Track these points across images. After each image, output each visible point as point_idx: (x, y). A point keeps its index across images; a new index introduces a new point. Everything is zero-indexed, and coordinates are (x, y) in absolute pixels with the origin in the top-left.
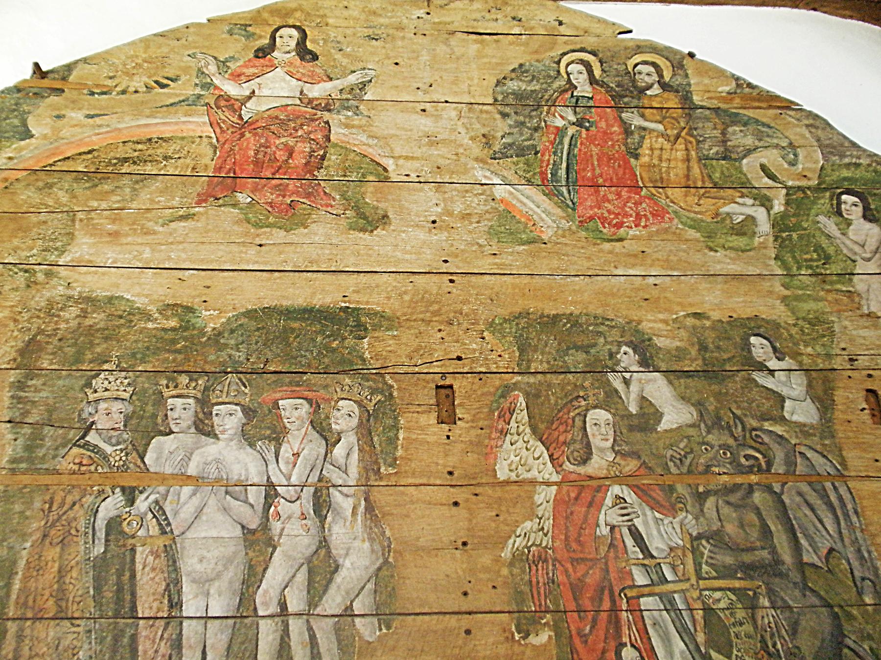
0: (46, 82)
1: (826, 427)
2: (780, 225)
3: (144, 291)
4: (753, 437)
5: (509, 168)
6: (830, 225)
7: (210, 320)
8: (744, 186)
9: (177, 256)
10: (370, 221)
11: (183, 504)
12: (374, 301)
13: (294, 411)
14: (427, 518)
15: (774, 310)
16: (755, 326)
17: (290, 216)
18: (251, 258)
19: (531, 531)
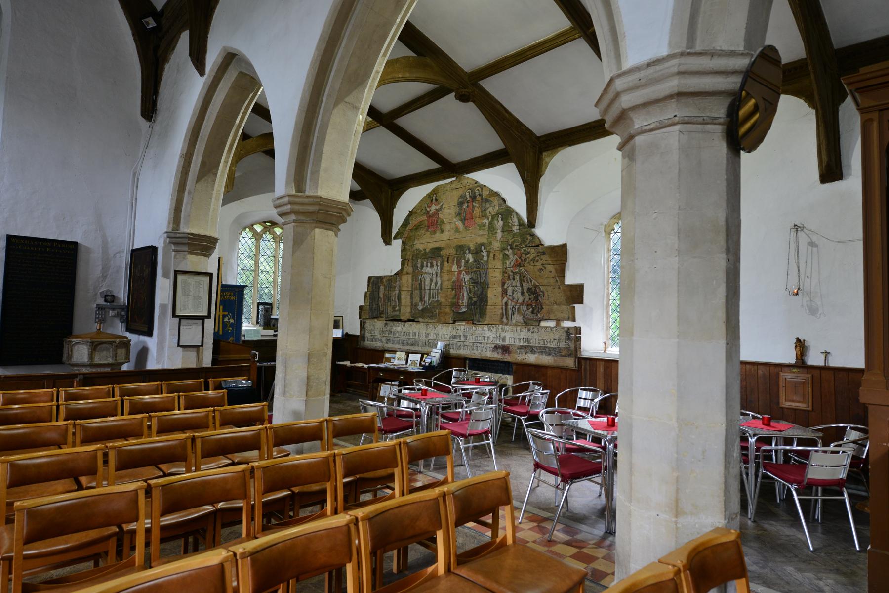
0: (411, 213)
1: (488, 261)
2: (490, 224)
3: (421, 247)
4: (479, 264)
5: (458, 218)
6: (496, 222)
7: (427, 250)
8: (486, 216)
9: (424, 241)
10: (442, 231)
11: (426, 276)
12: (442, 245)
13: (434, 263)
14: (446, 277)
15: (485, 241)
16: (482, 244)
17: (434, 232)
18: (431, 240)
19: (454, 278)
